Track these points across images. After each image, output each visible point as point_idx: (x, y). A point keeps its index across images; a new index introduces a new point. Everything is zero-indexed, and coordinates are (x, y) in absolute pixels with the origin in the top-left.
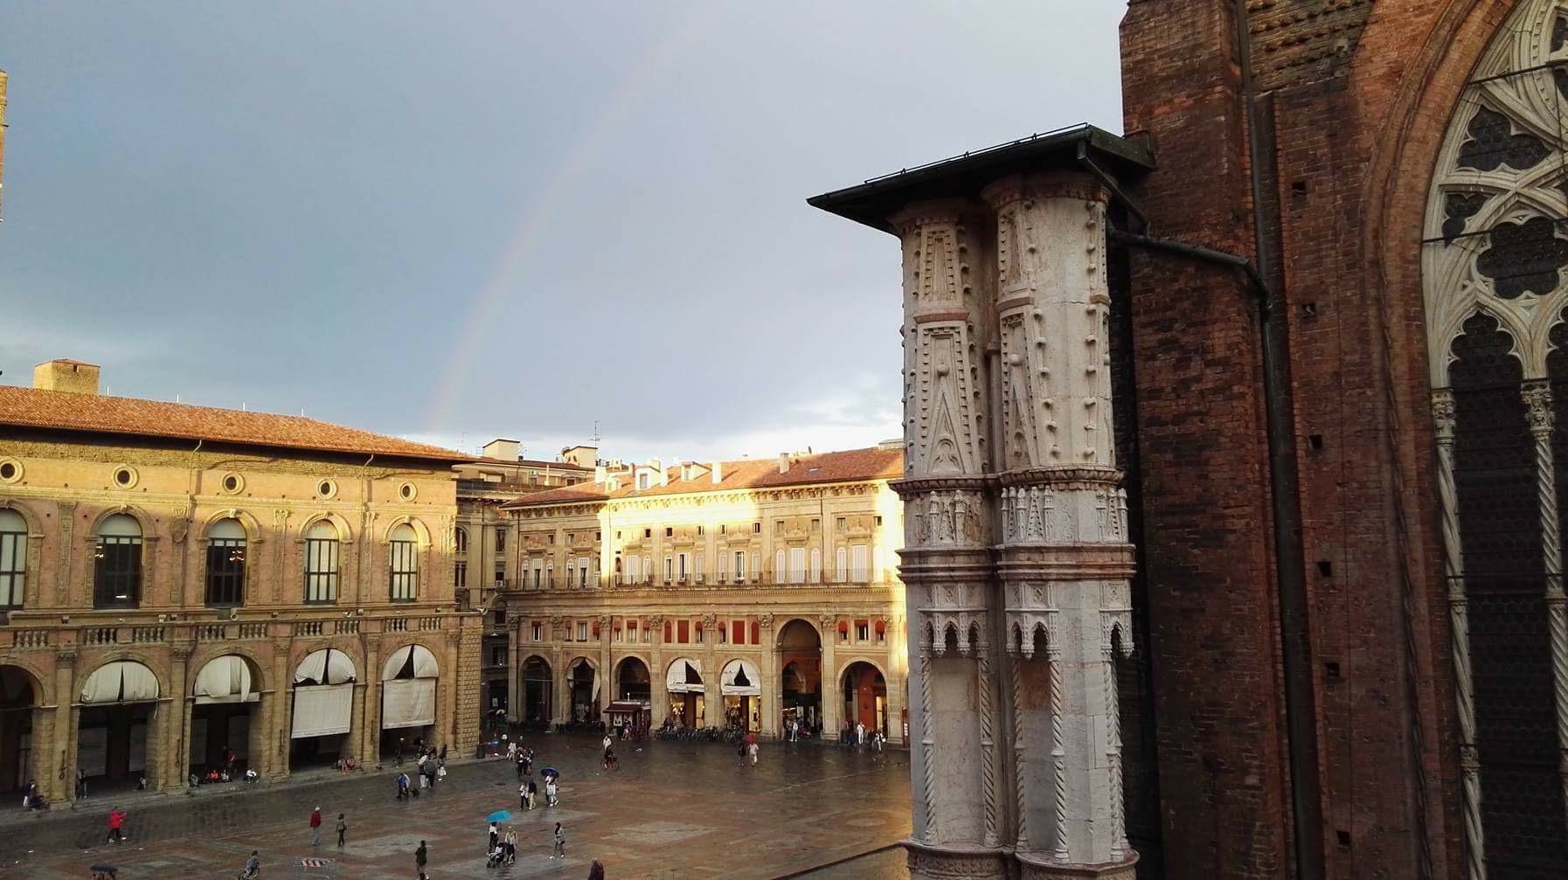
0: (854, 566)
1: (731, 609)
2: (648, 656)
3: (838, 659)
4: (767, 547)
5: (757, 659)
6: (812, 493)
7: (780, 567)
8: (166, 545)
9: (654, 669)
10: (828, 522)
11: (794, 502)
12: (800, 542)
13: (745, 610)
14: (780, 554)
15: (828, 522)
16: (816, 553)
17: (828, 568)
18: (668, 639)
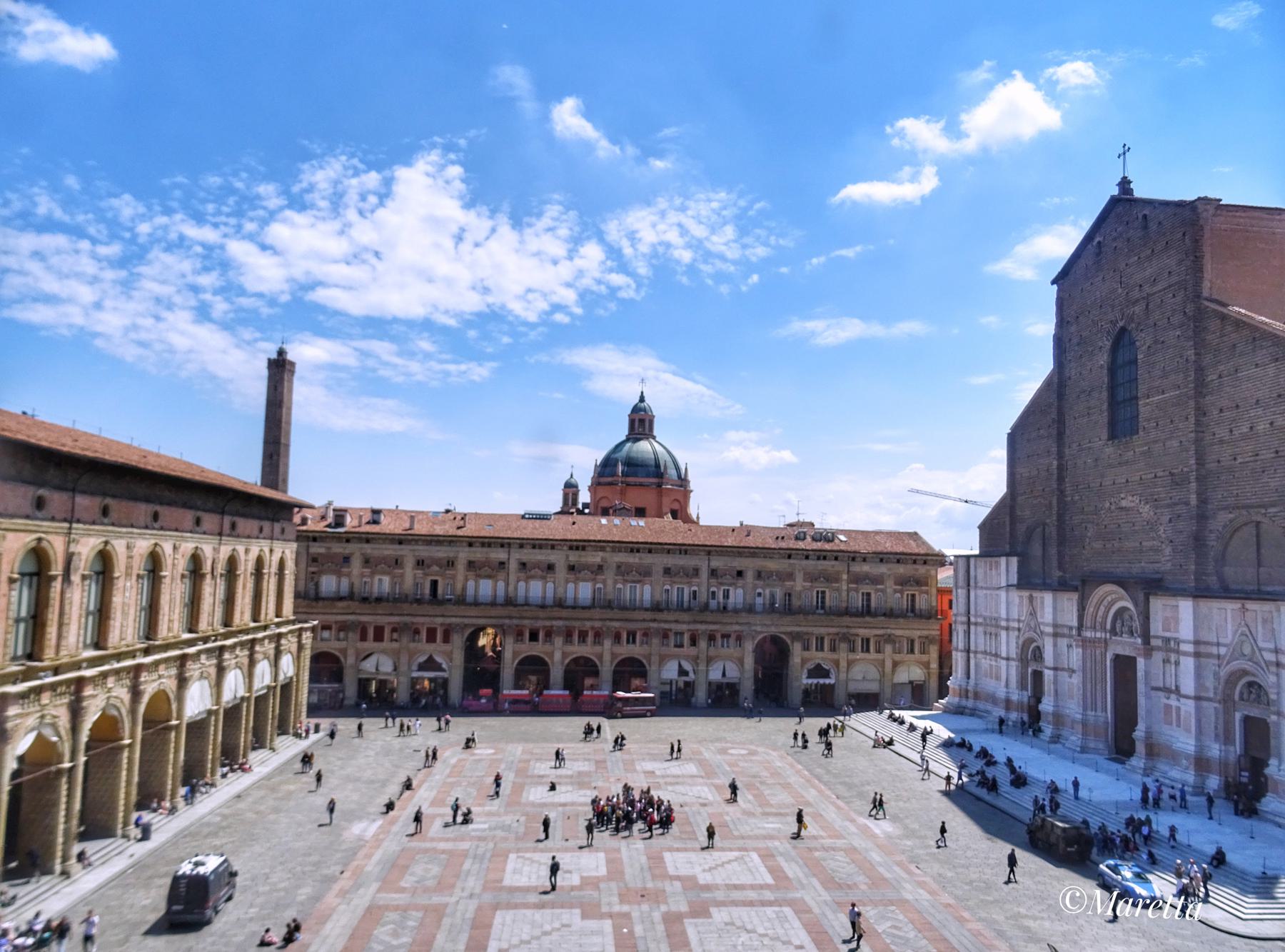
0: (531, 594)
1: (427, 620)
2: (344, 651)
3: (515, 654)
4: (460, 578)
5: (449, 656)
6: (502, 546)
7: (470, 591)
8: (135, 572)
9: (351, 660)
10: (513, 566)
11: (485, 549)
12: (489, 577)
13: (439, 620)
14: (471, 584)
15: (513, 566)
16: (501, 585)
17: (511, 593)
18: (363, 638)
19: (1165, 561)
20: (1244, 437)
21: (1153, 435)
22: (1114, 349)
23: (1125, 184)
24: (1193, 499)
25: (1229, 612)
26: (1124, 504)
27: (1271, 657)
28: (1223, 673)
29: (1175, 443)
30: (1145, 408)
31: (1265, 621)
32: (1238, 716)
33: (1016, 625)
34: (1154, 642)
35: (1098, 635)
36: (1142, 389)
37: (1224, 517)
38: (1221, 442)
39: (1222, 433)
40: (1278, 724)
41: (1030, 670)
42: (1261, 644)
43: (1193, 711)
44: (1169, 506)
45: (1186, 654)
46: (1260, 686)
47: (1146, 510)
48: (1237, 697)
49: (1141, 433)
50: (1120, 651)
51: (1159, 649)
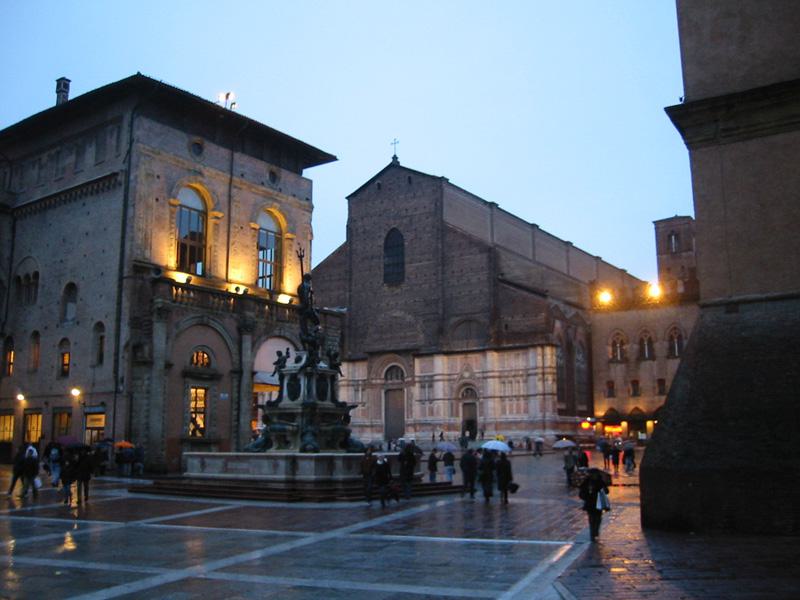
19: (421, 340)
22: (387, 239)
23: (395, 158)
24: (441, 312)
26: (395, 315)
28: (455, 386)
29: (427, 286)
30: (409, 268)
34: (417, 379)
35: (379, 381)
36: (407, 259)
37: (454, 320)
38: (453, 286)
40: (481, 404)
42: (476, 371)
46: (472, 390)
47: (409, 318)
48: (460, 396)
49: (406, 280)
51: (420, 382)
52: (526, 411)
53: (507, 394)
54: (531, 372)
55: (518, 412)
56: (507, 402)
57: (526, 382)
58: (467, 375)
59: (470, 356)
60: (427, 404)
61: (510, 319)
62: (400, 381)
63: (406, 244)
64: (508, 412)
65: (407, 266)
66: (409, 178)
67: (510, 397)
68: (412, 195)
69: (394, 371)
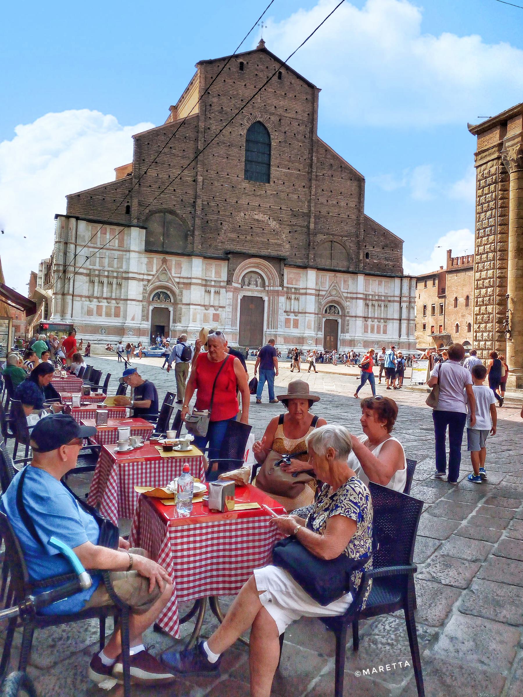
19: (285, 251)
20: (333, 205)
21: (281, 188)
22: (249, 130)
23: (262, 42)
25: (328, 277)
26: (256, 217)
27: (349, 295)
28: (323, 302)
29: (296, 197)
31: (345, 281)
32: (324, 320)
33: (146, 277)
38: (322, 204)
39: (323, 200)
40: (348, 320)
41: (151, 308)
43: (313, 319)
44: (290, 225)
45: (311, 294)
47: (273, 224)
50: (249, 294)
52: (385, 332)
53: (370, 316)
54: (389, 299)
55: (378, 332)
56: (370, 322)
57: (386, 306)
58: (334, 293)
59: (339, 275)
60: (292, 317)
61: (371, 249)
62: (259, 288)
63: (273, 144)
64: (369, 331)
65: (273, 169)
66: (280, 73)
67: (373, 318)
68: (283, 94)
69: (256, 276)
